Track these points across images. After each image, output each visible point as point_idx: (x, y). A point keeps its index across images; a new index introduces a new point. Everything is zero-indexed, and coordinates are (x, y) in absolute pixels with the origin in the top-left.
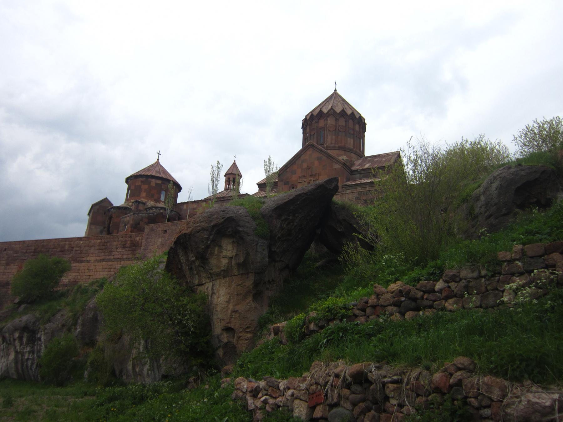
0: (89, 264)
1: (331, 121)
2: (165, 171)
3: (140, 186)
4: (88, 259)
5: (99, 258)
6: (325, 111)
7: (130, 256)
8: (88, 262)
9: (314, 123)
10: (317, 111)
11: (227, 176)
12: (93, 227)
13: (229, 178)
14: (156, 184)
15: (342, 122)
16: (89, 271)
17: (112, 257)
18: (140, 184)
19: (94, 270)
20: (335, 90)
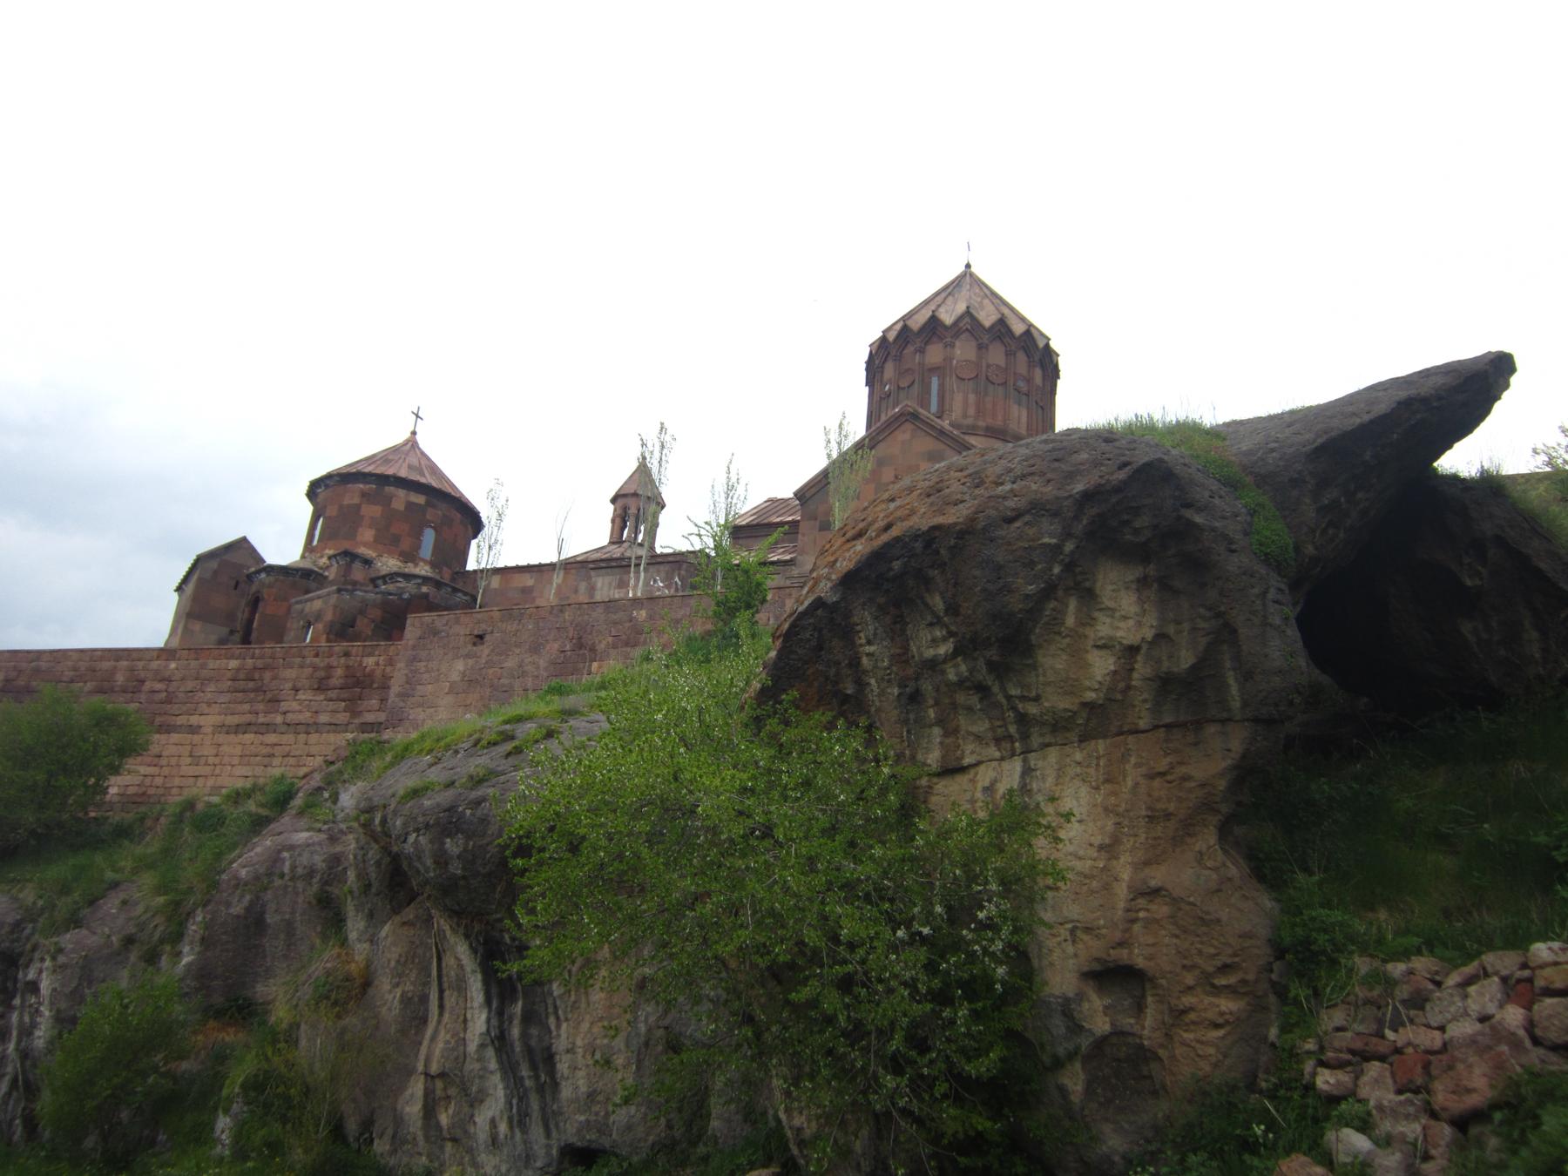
0: (196, 738)
1: (964, 351)
2: (434, 470)
3: (358, 507)
4: (194, 720)
5: (232, 720)
6: (947, 318)
7: (343, 717)
8: (194, 730)
9: (901, 358)
10: (925, 315)
11: (620, 502)
12: (197, 626)
13: (625, 509)
14: (410, 506)
15: (996, 355)
16: (196, 760)
17: (279, 719)
18: (356, 500)
19: (211, 760)
20: (968, 266)
